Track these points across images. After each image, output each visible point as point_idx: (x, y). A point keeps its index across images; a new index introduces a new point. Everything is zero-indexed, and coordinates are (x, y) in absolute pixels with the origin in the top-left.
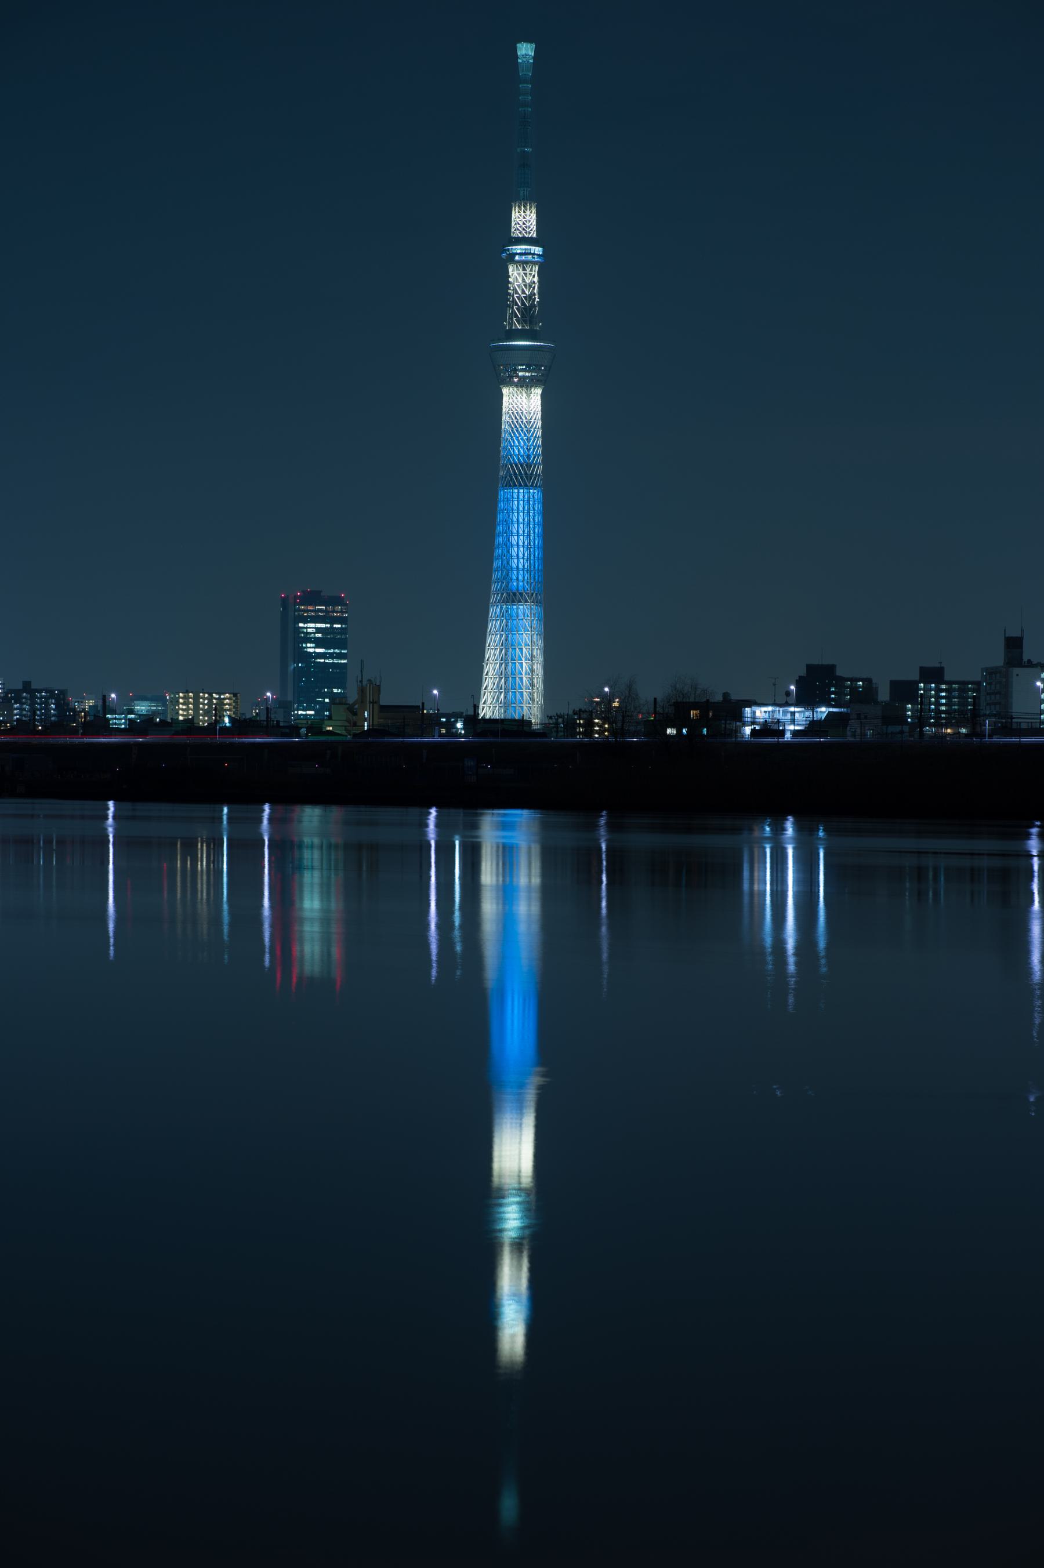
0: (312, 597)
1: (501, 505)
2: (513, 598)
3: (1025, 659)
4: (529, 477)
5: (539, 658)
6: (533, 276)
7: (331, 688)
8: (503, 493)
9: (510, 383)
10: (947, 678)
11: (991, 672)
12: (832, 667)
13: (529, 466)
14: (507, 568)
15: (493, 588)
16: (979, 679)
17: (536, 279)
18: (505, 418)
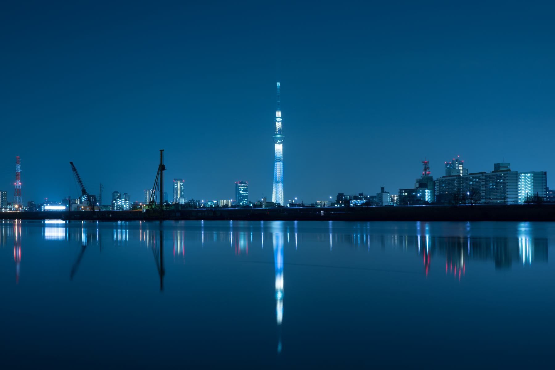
0: (241, 183)
1: (275, 165)
2: (278, 182)
3: (385, 191)
4: (280, 160)
5: (283, 193)
6: (280, 124)
7: (245, 199)
8: (276, 163)
9: (277, 143)
10: (363, 195)
11: (379, 194)
12: (343, 194)
13: (280, 158)
14: (276, 177)
15: (274, 180)
16: (376, 195)
17: (281, 124)
18: (276, 150)
